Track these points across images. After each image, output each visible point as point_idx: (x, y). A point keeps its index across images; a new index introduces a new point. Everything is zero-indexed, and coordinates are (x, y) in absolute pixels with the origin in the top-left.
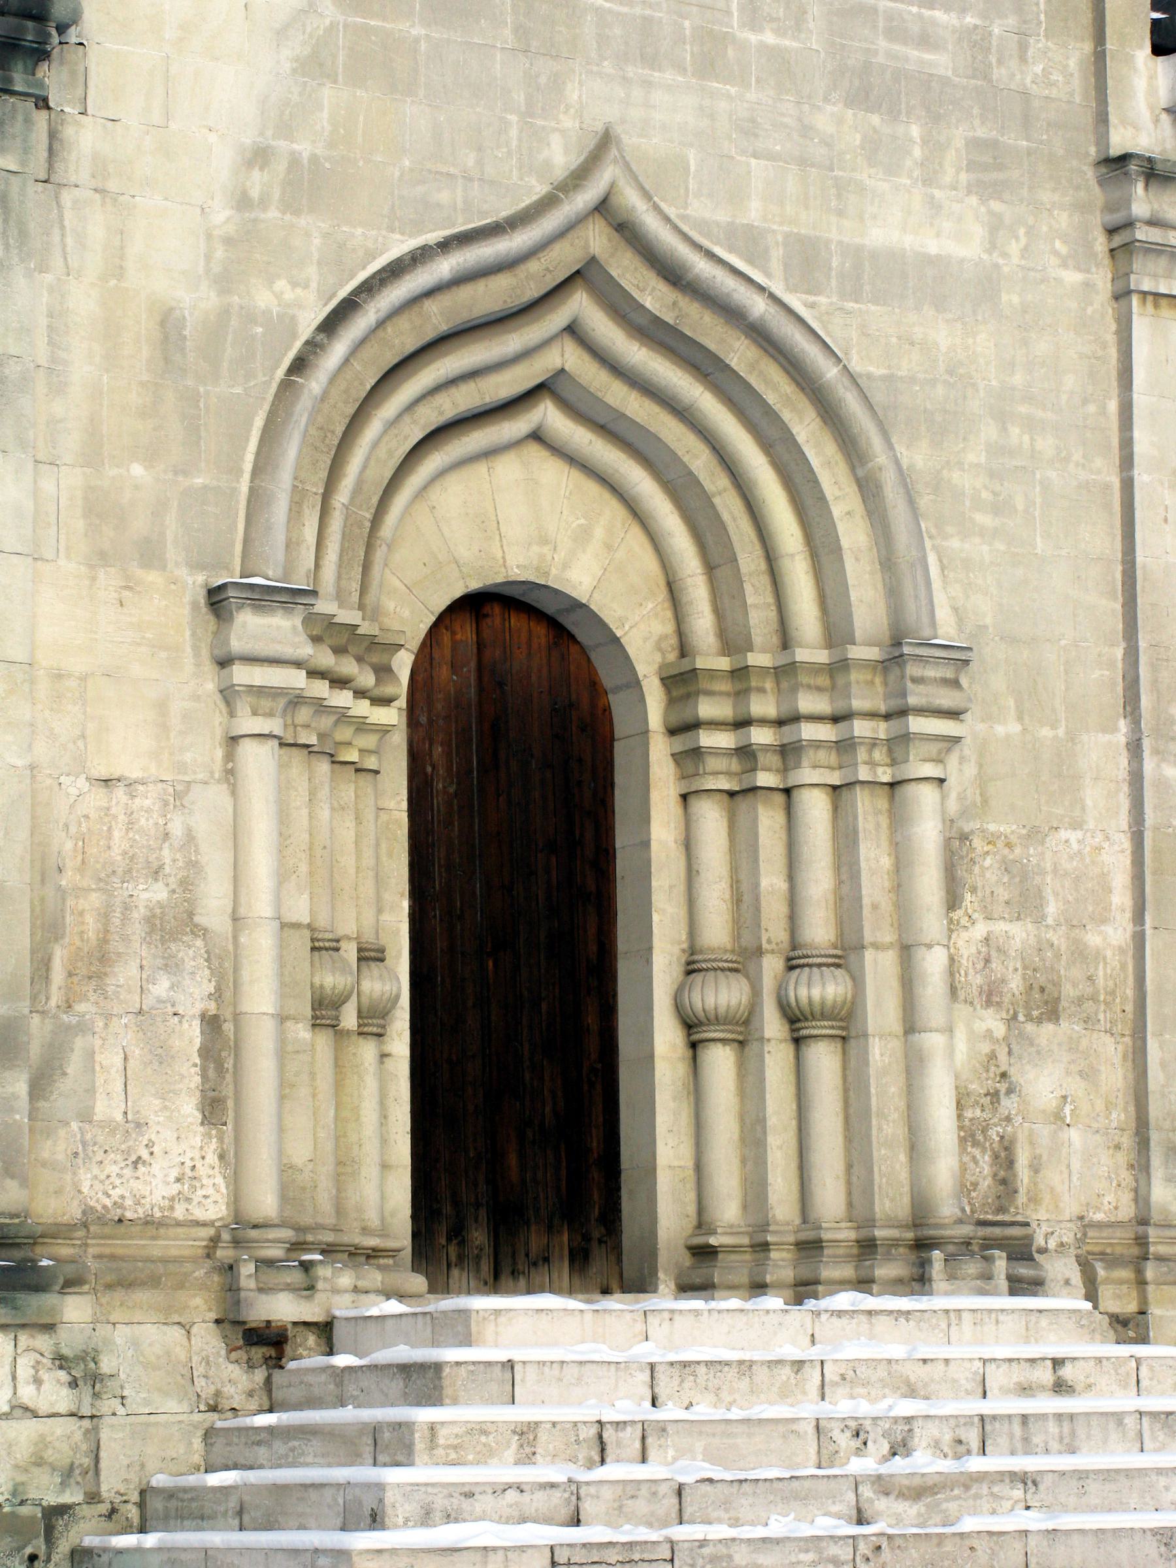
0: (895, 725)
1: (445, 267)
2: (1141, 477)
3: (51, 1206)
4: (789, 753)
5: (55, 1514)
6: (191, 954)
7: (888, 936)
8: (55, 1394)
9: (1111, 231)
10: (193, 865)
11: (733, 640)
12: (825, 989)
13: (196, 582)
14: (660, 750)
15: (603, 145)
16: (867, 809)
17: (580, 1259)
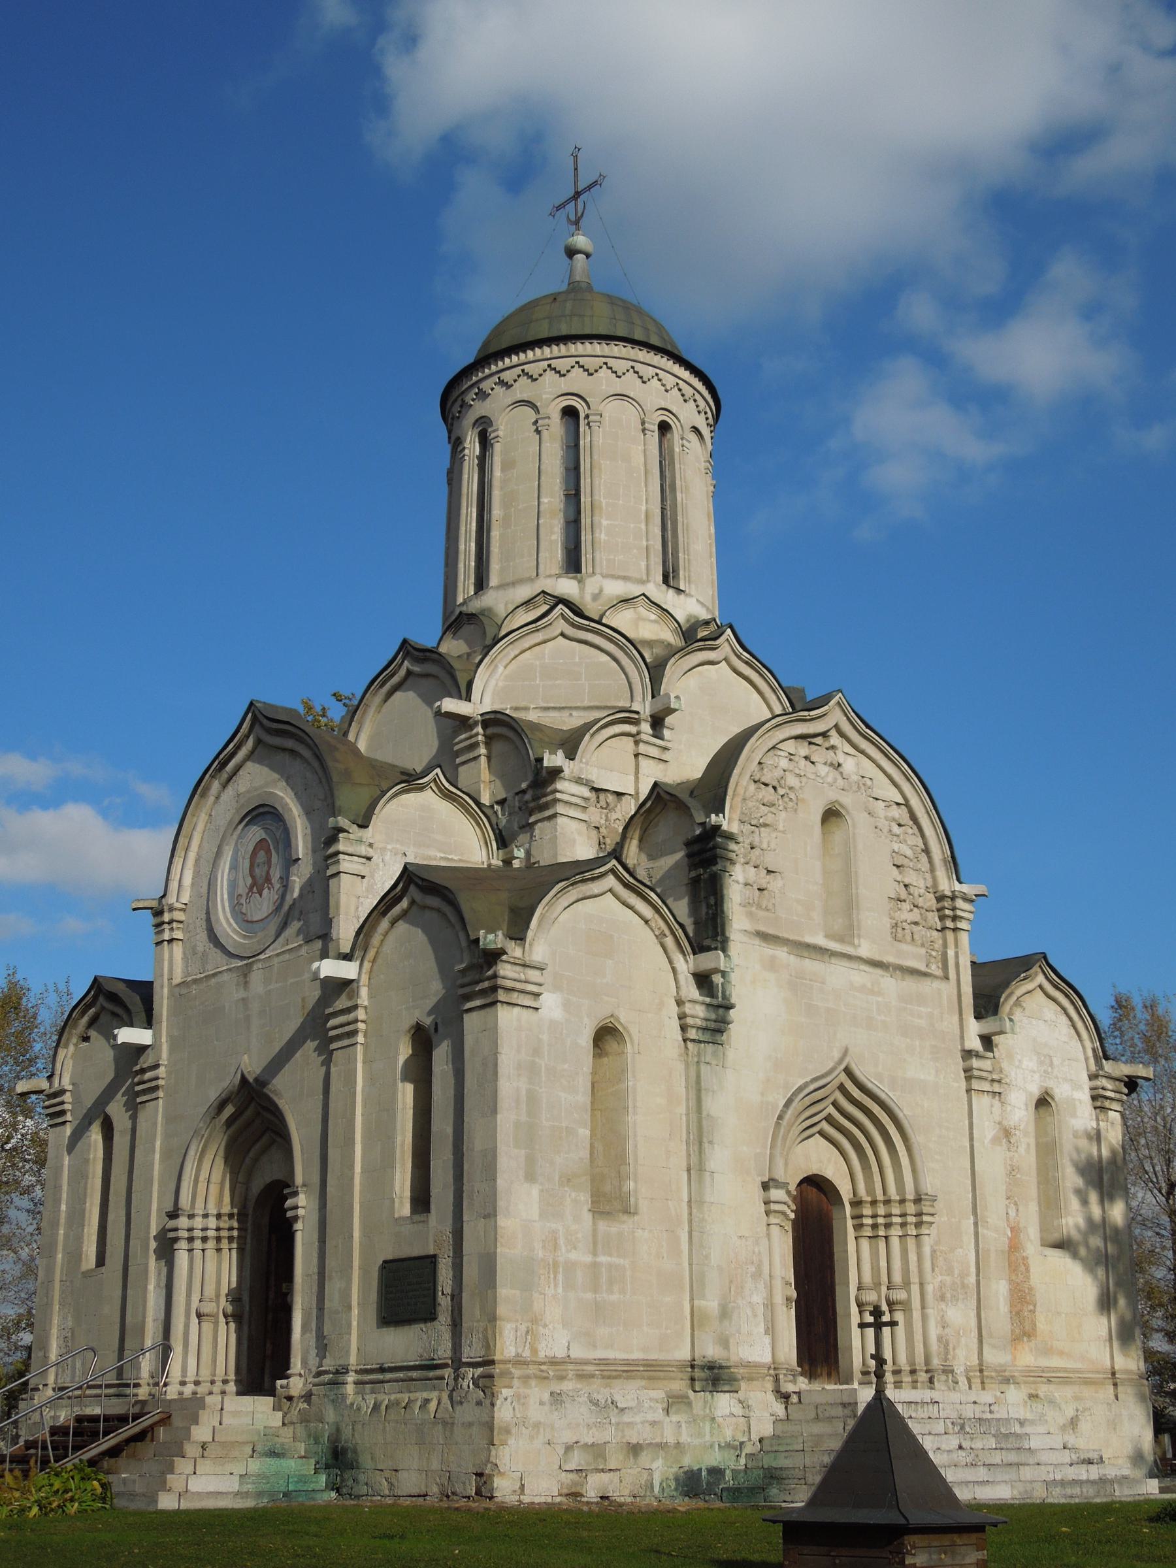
0: (918, 1218)
1: (812, 1087)
2: (976, 1144)
3: (734, 1358)
4: (888, 1226)
5: (742, 1444)
7: (917, 1280)
8: (738, 1410)
9: (965, 1071)
10: (760, 1261)
11: (870, 1190)
13: (759, 1180)
14: (850, 1223)
15: (846, 1052)
16: (911, 1242)
17: (829, 1375)
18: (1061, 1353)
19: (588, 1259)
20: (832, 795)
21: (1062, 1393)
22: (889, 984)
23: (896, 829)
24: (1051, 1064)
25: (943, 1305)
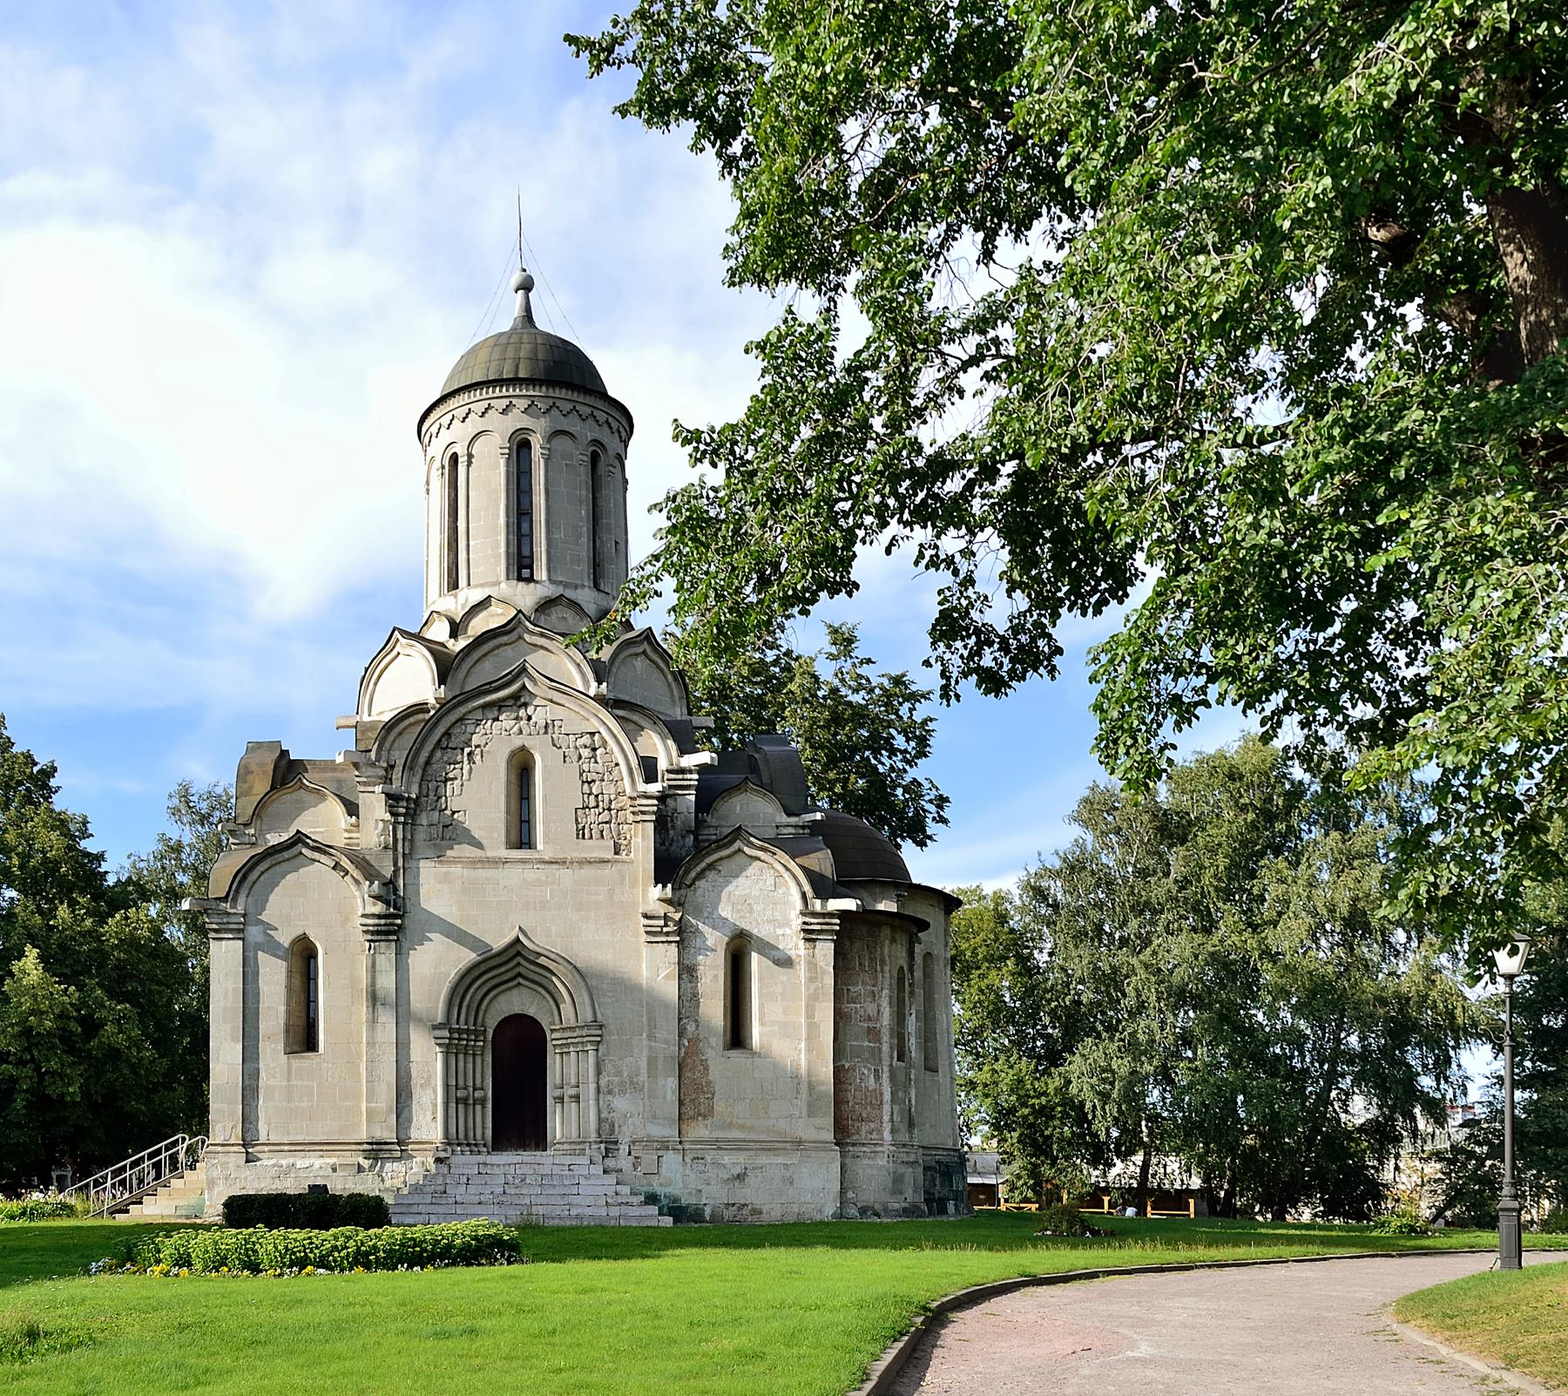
6: (430, 1091)
12: (573, 1091)
18: (742, 1127)
19: (284, 1083)
20: (518, 742)
21: (727, 1159)
22: (565, 874)
23: (586, 753)
24: (751, 911)
25: (609, 1097)
